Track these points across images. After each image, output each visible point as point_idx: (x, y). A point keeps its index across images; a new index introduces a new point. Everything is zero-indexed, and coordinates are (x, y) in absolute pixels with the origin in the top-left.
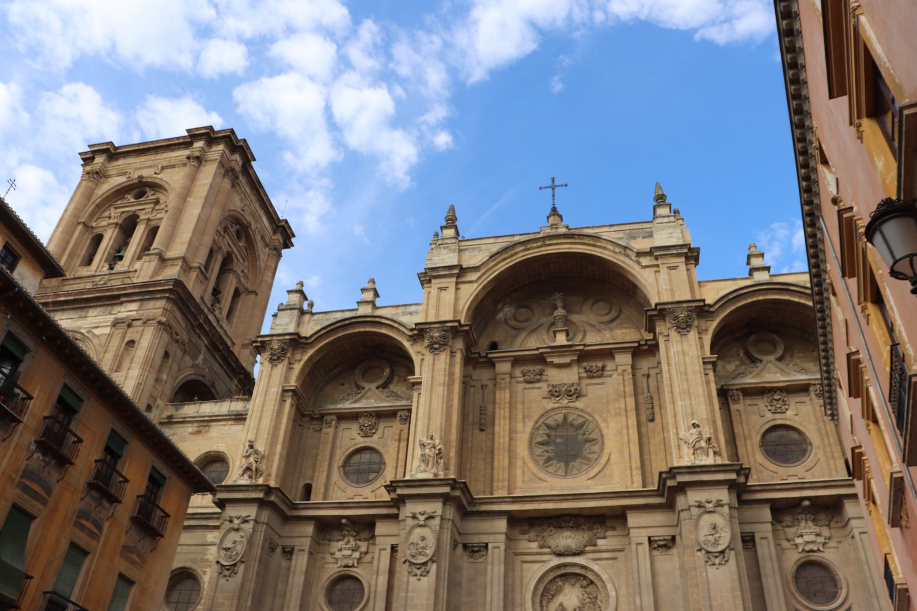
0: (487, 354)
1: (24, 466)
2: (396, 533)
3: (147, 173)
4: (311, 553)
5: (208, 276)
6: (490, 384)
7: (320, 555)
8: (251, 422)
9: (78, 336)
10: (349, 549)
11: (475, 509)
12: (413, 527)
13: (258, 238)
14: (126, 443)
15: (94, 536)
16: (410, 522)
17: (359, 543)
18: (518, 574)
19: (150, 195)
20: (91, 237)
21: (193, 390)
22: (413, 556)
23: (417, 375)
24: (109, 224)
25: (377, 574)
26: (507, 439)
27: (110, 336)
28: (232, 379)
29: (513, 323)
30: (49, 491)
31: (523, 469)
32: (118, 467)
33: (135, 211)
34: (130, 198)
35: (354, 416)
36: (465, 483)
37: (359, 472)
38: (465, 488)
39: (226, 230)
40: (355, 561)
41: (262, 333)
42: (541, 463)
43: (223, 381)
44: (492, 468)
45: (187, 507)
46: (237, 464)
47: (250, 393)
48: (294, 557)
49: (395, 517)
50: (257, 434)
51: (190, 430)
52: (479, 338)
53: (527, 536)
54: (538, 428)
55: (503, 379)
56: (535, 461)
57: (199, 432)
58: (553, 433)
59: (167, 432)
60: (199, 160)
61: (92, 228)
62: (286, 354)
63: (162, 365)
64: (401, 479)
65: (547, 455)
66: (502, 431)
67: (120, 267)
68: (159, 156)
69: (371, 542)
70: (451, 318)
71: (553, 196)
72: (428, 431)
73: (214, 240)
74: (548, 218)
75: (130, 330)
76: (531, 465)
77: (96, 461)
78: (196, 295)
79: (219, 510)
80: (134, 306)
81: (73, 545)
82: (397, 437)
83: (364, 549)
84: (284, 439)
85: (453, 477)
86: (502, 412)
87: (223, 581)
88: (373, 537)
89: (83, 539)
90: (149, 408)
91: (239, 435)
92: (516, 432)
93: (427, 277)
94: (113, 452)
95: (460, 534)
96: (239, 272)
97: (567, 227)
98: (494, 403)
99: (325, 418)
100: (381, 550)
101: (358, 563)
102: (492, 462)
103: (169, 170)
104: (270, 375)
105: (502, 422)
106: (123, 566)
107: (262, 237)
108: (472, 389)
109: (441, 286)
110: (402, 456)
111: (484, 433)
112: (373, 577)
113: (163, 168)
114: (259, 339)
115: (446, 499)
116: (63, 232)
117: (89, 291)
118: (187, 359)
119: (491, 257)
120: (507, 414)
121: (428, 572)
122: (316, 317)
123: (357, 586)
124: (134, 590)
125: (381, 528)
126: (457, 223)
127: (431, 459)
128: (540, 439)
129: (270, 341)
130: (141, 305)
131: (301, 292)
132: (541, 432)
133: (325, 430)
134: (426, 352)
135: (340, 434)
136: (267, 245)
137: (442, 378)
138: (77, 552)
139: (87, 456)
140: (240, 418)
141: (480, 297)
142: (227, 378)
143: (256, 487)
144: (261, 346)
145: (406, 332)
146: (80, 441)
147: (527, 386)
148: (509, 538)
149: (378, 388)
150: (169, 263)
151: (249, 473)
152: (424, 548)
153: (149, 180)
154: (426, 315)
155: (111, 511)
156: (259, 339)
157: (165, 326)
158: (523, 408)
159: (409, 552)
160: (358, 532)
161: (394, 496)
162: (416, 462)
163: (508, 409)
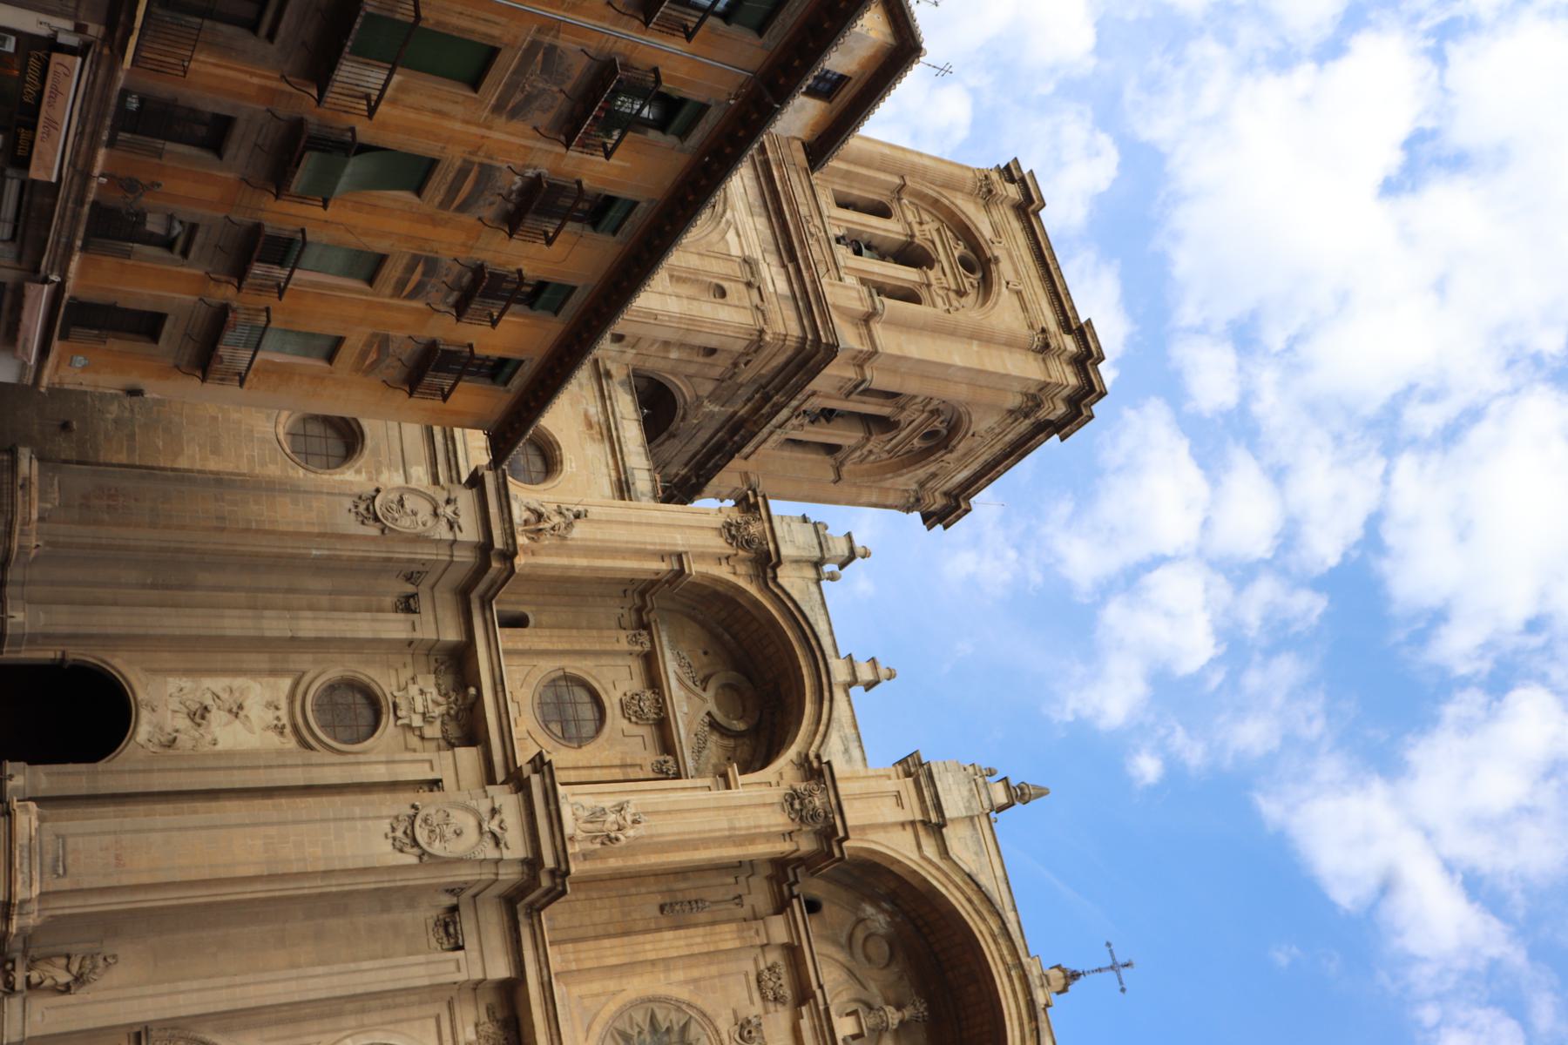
0: (798, 897)
1: (498, 164)
2: (462, 784)
3: (1004, 270)
4: (411, 643)
5: (853, 396)
6: (745, 911)
7: (409, 659)
8: (620, 509)
9: (719, 208)
10: (426, 707)
11: (521, 917)
12: (476, 813)
13: (932, 468)
14: (556, 313)
15: (398, 290)
16: (484, 806)
17: (438, 723)
18: (415, 1011)
19: (970, 281)
20: (884, 199)
21: (658, 405)
22: (425, 821)
23: (742, 779)
24: (910, 224)
25: (387, 762)
26: (652, 956)
27: (728, 257)
28: (686, 465)
29: (860, 935)
30: (462, 208)
31: (604, 993)
32: (514, 307)
34: (959, 250)
35: (654, 681)
36: (564, 892)
37: (559, 704)
38: (556, 894)
39: (935, 412)
40: (406, 721)
41: (772, 503)
42: (617, 1024)
43: (680, 451)
44: (596, 938)
45: (463, 426)
46: (545, 497)
47: (668, 498)
48: (402, 616)
49: (490, 779)
50: (599, 521)
51: (592, 411)
52: (825, 878)
53: (484, 1018)
54: (679, 1009)
55: (757, 933)
56: (621, 1013)
57: (590, 425)
58: (675, 1037)
59: (583, 375)
61: (899, 199)
62: (743, 548)
63: (692, 347)
64: (557, 780)
65: (635, 1032)
66: (664, 945)
67: (843, 253)
68: (1037, 283)
69: (443, 743)
70: (849, 823)
71: (1100, 970)
72: (646, 813)
73: (915, 397)
74: (1058, 967)
75: (742, 287)
76: (612, 1007)
77: (520, 271)
78: (817, 384)
79: (464, 478)
80: (782, 286)
81: (382, 259)
82: (629, 761)
83: (430, 731)
84: (597, 569)
85: (573, 869)
86: (699, 940)
87: (348, 503)
88: (451, 746)
89: (392, 272)
90: (618, 338)
91: (595, 494)
92: (667, 970)
93: (915, 769)
94: (537, 295)
95: (475, 896)
96: (869, 446)
97: (1047, 1005)
98: (713, 923)
99: (644, 633)
100: (431, 762)
101: (403, 726)
102: (609, 936)
103: (1017, 304)
104: (702, 528)
105: (682, 943)
106: (355, 340)
107: (934, 475)
108: (732, 880)
109: (903, 795)
110: (597, 774)
111: (658, 913)
112: (383, 755)
113: (1019, 293)
114: (760, 499)
115: (533, 863)
116: (883, 155)
117: (795, 213)
118: (709, 387)
119: (969, 876)
120: (696, 950)
121: (401, 851)
122: (813, 588)
123: (364, 730)
124: (322, 364)
125: (468, 757)
126: (1018, 805)
127: (598, 826)
128: (660, 1016)
130: (786, 297)
131: (852, 556)
132: (674, 1016)
133: (623, 634)
134: (784, 789)
135: (620, 662)
136: (922, 485)
137: (743, 824)
138: (370, 267)
139: (527, 257)
140: (623, 488)
141: (895, 868)
142: (686, 457)
143: (511, 534)
144: (749, 504)
145: (813, 748)
146: (549, 242)
147: (753, 978)
148: (476, 986)
149: (709, 714)
150: (864, 331)
151: (533, 518)
153: (995, 275)
154: (848, 779)
155: (442, 308)
156: (760, 499)
157: (757, 342)
158: (712, 977)
159: (432, 811)
160: (456, 718)
161: (527, 770)
162: (589, 802)
163: (705, 949)
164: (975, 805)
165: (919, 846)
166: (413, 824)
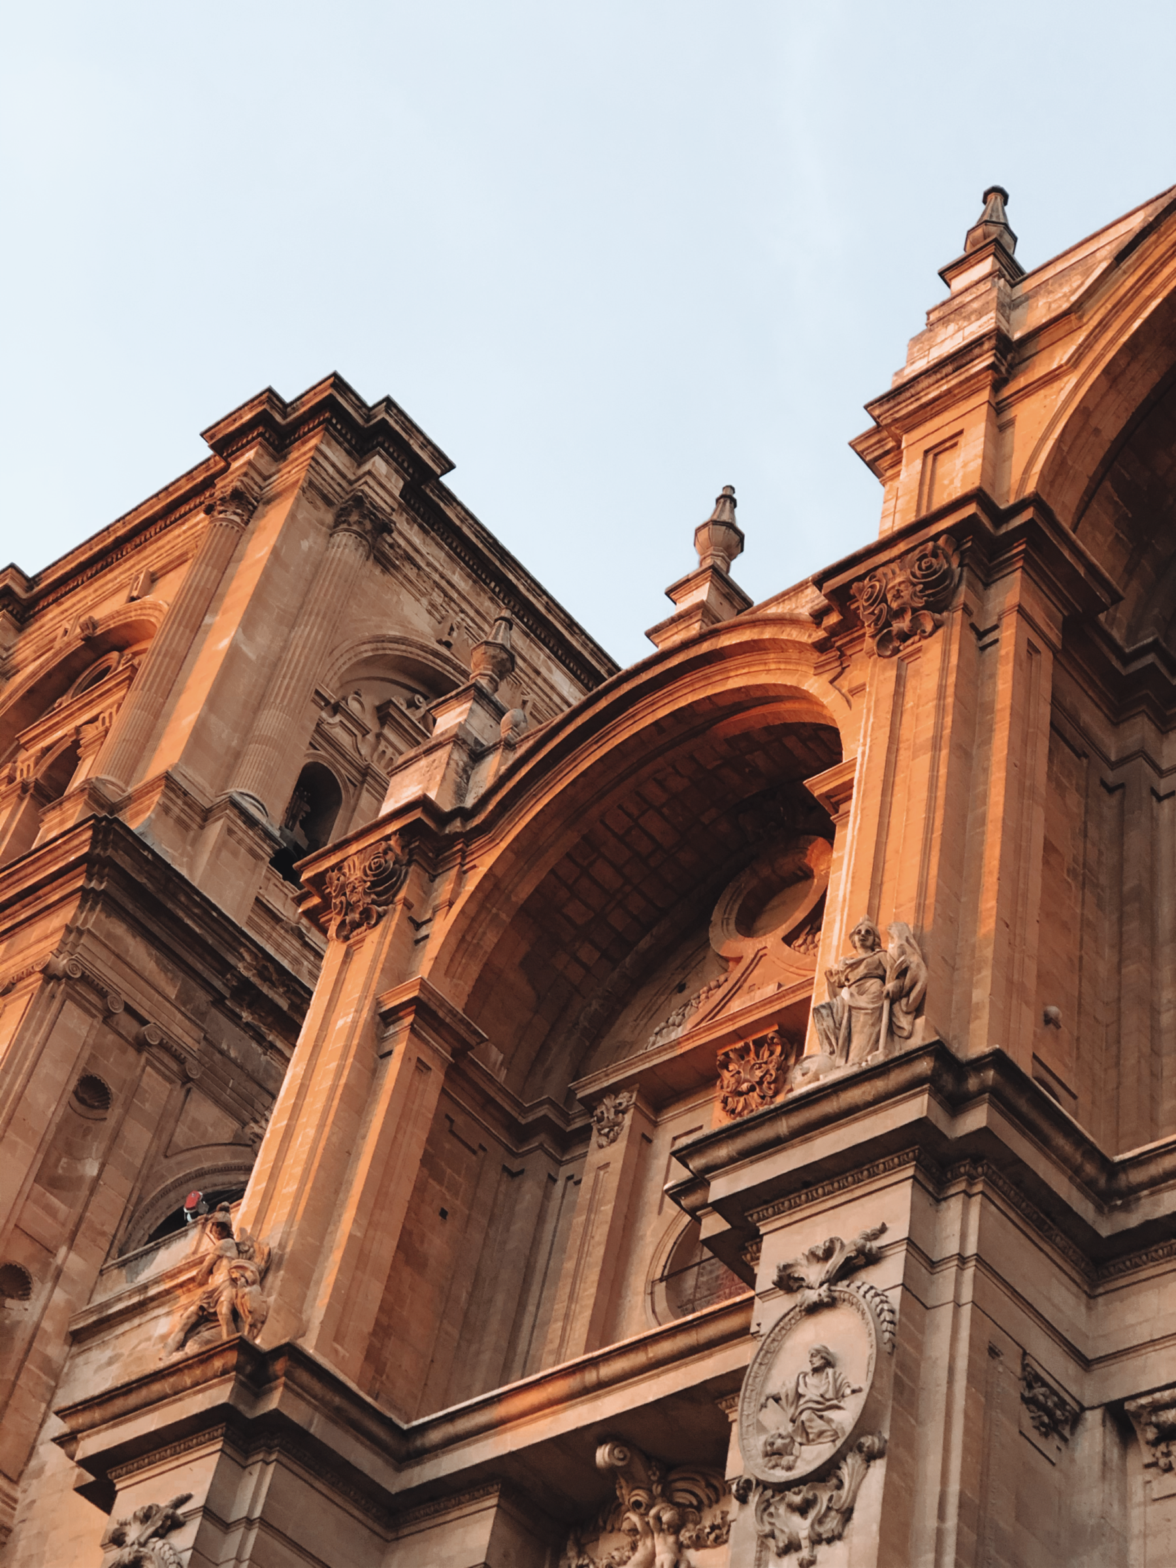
11: (1133, 1220)
12: (784, 1326)
33: (78, 730)
36: (998, 1060)
39: (384, 713)
60: (247, 503)
62: (395, 889)
95: (1087, 1364)
115: (934, 1162)
119: (1121, 256)
121: (847, 1514)
129: (338, 866)
137: (931, 722)
141: (1111, 426)
149: (788, 940)
152: (824, 1405)
159: (763, 1438)
161: (713, 1225)
164: (975, 305)
165: (1052, 377)
166: (782, 1488)
